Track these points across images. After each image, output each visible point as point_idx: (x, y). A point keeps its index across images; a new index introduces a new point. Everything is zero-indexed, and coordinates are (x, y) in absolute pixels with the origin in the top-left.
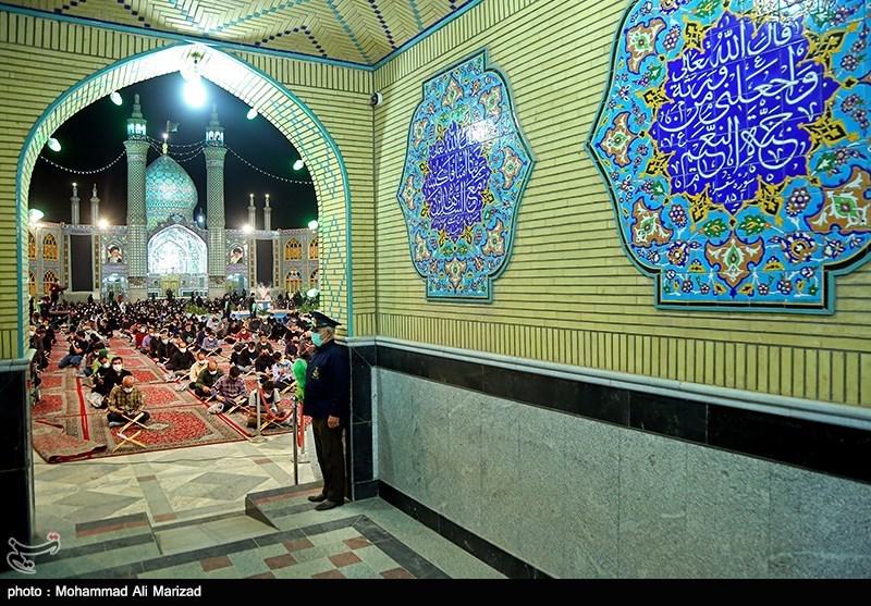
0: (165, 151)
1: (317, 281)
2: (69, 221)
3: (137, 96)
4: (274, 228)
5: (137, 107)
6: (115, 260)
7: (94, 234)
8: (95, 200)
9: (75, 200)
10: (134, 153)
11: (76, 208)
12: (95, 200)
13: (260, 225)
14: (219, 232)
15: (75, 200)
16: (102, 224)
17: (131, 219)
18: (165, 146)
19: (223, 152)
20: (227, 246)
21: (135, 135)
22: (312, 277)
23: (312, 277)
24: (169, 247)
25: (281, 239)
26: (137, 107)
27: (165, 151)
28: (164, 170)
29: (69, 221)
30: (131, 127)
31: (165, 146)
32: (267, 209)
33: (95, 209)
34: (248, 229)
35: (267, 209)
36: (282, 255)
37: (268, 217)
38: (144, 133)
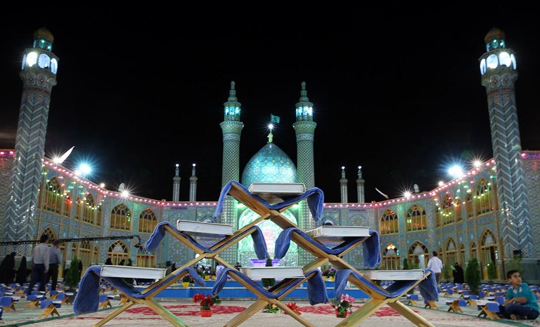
0: (270, 140)
5: (233, 92)
9: (177, 179)
15: (177, 179)
18: (270, 136)
19: (312, 126)
26: (233, 92)
27: (270, 140)
28: (267, 155)
29: (170, 198)
30: (227, 111)
31: (270, 136)
35: (360, 181)
37: (361, 189)
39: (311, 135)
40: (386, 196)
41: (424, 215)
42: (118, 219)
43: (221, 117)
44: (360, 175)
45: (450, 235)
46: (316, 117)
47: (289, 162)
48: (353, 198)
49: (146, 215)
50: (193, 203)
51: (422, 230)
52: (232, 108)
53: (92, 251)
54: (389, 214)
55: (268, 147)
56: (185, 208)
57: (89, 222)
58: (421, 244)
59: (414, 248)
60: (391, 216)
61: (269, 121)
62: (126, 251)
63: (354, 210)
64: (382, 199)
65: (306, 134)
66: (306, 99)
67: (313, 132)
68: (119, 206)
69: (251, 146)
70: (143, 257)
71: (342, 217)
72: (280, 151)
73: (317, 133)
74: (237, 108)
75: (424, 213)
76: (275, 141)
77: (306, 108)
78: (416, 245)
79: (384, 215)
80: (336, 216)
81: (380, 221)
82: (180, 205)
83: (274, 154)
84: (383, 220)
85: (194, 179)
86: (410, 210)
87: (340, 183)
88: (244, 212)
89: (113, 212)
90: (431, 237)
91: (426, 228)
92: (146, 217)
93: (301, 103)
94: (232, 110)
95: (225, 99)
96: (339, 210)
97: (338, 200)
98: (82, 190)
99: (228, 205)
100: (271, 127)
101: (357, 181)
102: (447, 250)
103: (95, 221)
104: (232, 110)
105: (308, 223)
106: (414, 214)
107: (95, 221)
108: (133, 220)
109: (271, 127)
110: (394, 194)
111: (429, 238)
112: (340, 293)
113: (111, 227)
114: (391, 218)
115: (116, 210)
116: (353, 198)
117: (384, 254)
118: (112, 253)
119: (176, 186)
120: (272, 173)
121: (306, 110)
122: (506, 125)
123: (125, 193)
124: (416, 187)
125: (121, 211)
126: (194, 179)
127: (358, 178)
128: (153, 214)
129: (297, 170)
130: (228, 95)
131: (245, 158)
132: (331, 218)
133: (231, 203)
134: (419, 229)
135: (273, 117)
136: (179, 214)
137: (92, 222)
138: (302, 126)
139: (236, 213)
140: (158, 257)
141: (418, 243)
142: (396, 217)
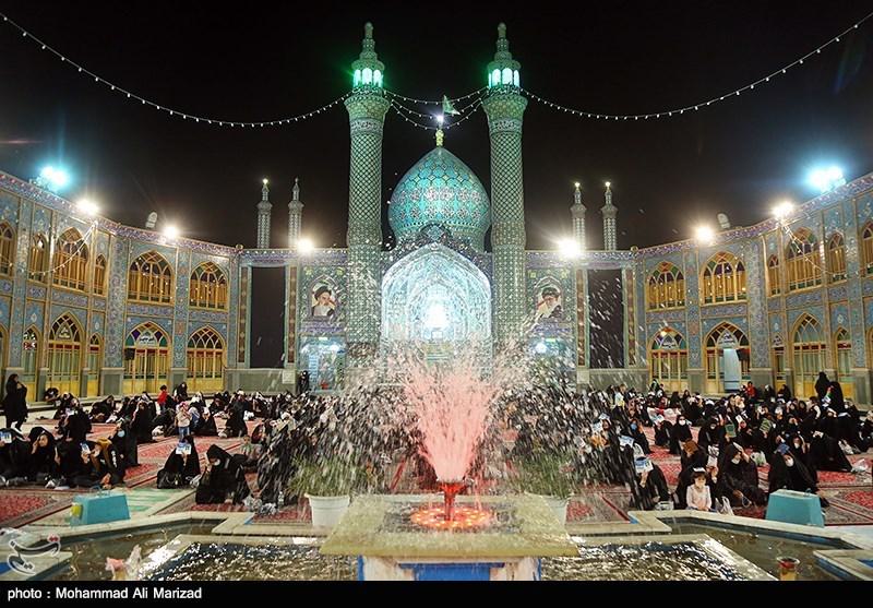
0: (439, 142)
1: (721, 352)
2: (251, 243)
4: (623, 245)
6: (323, 311)
7: (289, 263)
8: (295, 206)
9: (265, 206)
10: (363, 121)
11: (264, 222)
12: (295, 206)
13: (597, 242)
15: (265, 206)
16: (304, 245)
17: (353, 237)
18: (439, 135)
19: (519, 105)
20: (529, 290)
21: (362, 87)
22: (710, 343)
23: (710, 343)
25: (638, 270)
27: (439, 142)
29: (251, 243)
31: (439, 135)
32: (609, 208)
33: (295, 219)
34: (570, 249)
35: (609, 208)
36: (641, 300)
37: (610, 226)
38: (380, 85)
39: (518, 122)
41: (740, 273)
42: (145, 281)
43: (346, 88)
45: (812, 312)
47: (472, 179)
49: (205, 274)
52: (367, 71)
53: (84, 344)
54: (665, 270)
55: (436, 154)
57: (74, 286)
58: (732, 328)
59: (716, 335)
60: (668, 274)
62: (164, 343)
65: (507, 124)
66: (504, 54)
67: (521, 117)
68: (146, 256)
69: (403, 150)
72: (457, 160)
73: (529, 118)
74: (377, 72)
75: (741, 268)
76: (446, 144)
77: (507, 72)
78: (721, 329)
83: (445, 167)
86: (711, 264)
89: (134, 267)
90: (754, 314)
91: (745, 298)
93: (496, 63)
94: (367, 76)
95: (354, 53)
100: (440, 119)
102: (796, 341)
103: (90, 286)
104: (367, 76)
105: (512, 287)
106: (718, 271)
107: (90, 286)
108: (179, 286)
109: (440, 119)
111: (751, 316)
112: (627, 460)
113: (130, 297)
114: (670, 278)
115: (140, 264)
119: (263, 220)
121: (503, 76)
123: (170, 234)
127: (605, 204)
134: (717, 300)
137: (81, 288)
138: (500, 104)
141: (727, 325)
142: (680, 277)
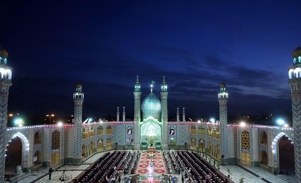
0: (152, 91)
3: (138, 76)
10: (137, 95)
14: (164, 122)
18: (152, 90)
19: (166, 94)
24: (151, 127)
27: (152, 91)
29: (116, 120)
31: (152, 90)
37: (184, 116)
40: (191, 120)
42: (99, 131)
43: (133, 90)
44: (184, 111)
46: (169, 90)
48: (181, 120)
50: (124, 122)
51: (203, 135)
56: (121, 124)
61: (151, 83)
62: (102, 141)
63: (181, 124)
64: (190, 121)
66: (164, 83)
70: (108, 142)
71: (177, 126)
73: (169, 95)
75: (204, 129)
79: (192, 127)
80: (175, 126)
81: (190, 128)
82: (120, 123)
84: (191, 128)
85: (124, 113)
87: (176, 114)
88: (142, 125)
89: (98, 129)
92: (108, 128)
96: (176, 124)
97: (176, 121)
98: (90, 127)
99: (136, 129)
101: (183, 113)
106: (201, 129)
109: (152, 86)
110: (195, 120)
116: (181, 120)
117: (191, 140)
118: (98, 143)
120: (153, 106)
122: (223, 114)
124: (202, 119)
125: (100, 128)
126: (124, 113)
128: (110, 127)
129: (161, 103)
130: (136, 81)
131: (142, 99)
132: (173, 127)
133: (138, 122)
135: (152, 81)
136: (119, 126)
139: (139, 126)
140: (113, 141)
